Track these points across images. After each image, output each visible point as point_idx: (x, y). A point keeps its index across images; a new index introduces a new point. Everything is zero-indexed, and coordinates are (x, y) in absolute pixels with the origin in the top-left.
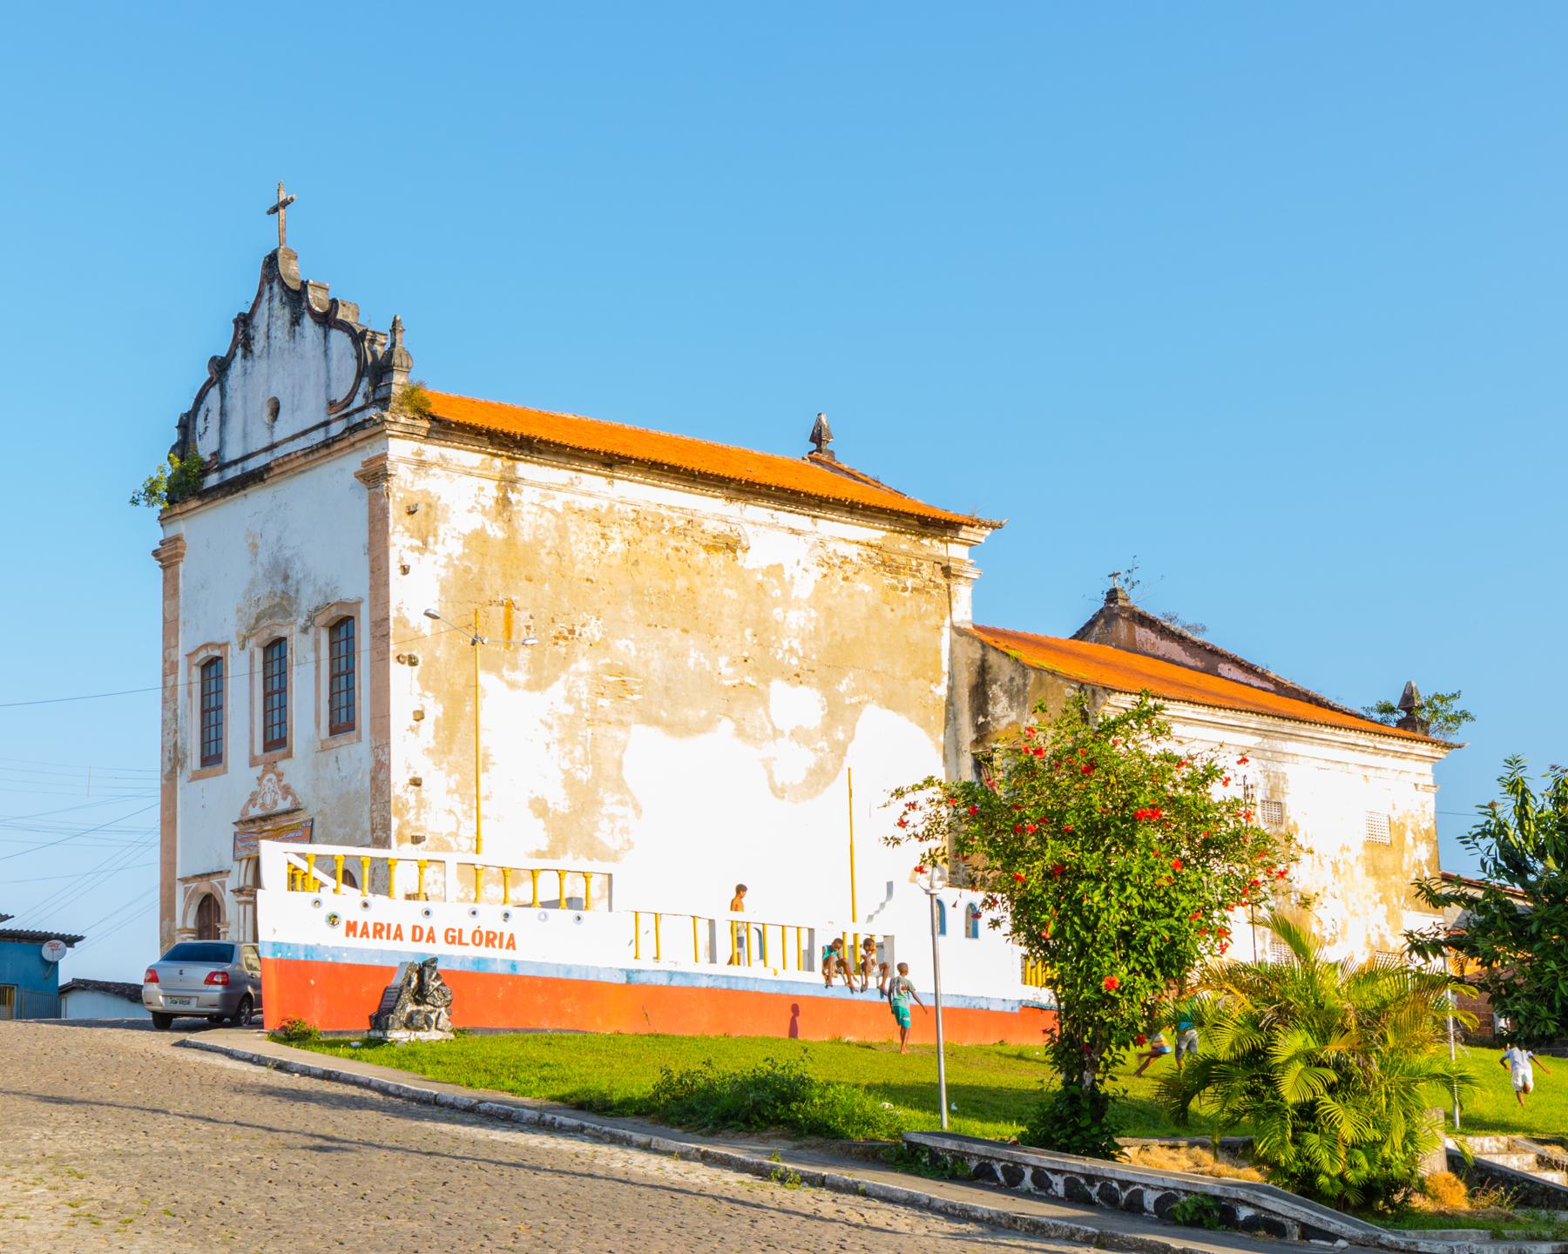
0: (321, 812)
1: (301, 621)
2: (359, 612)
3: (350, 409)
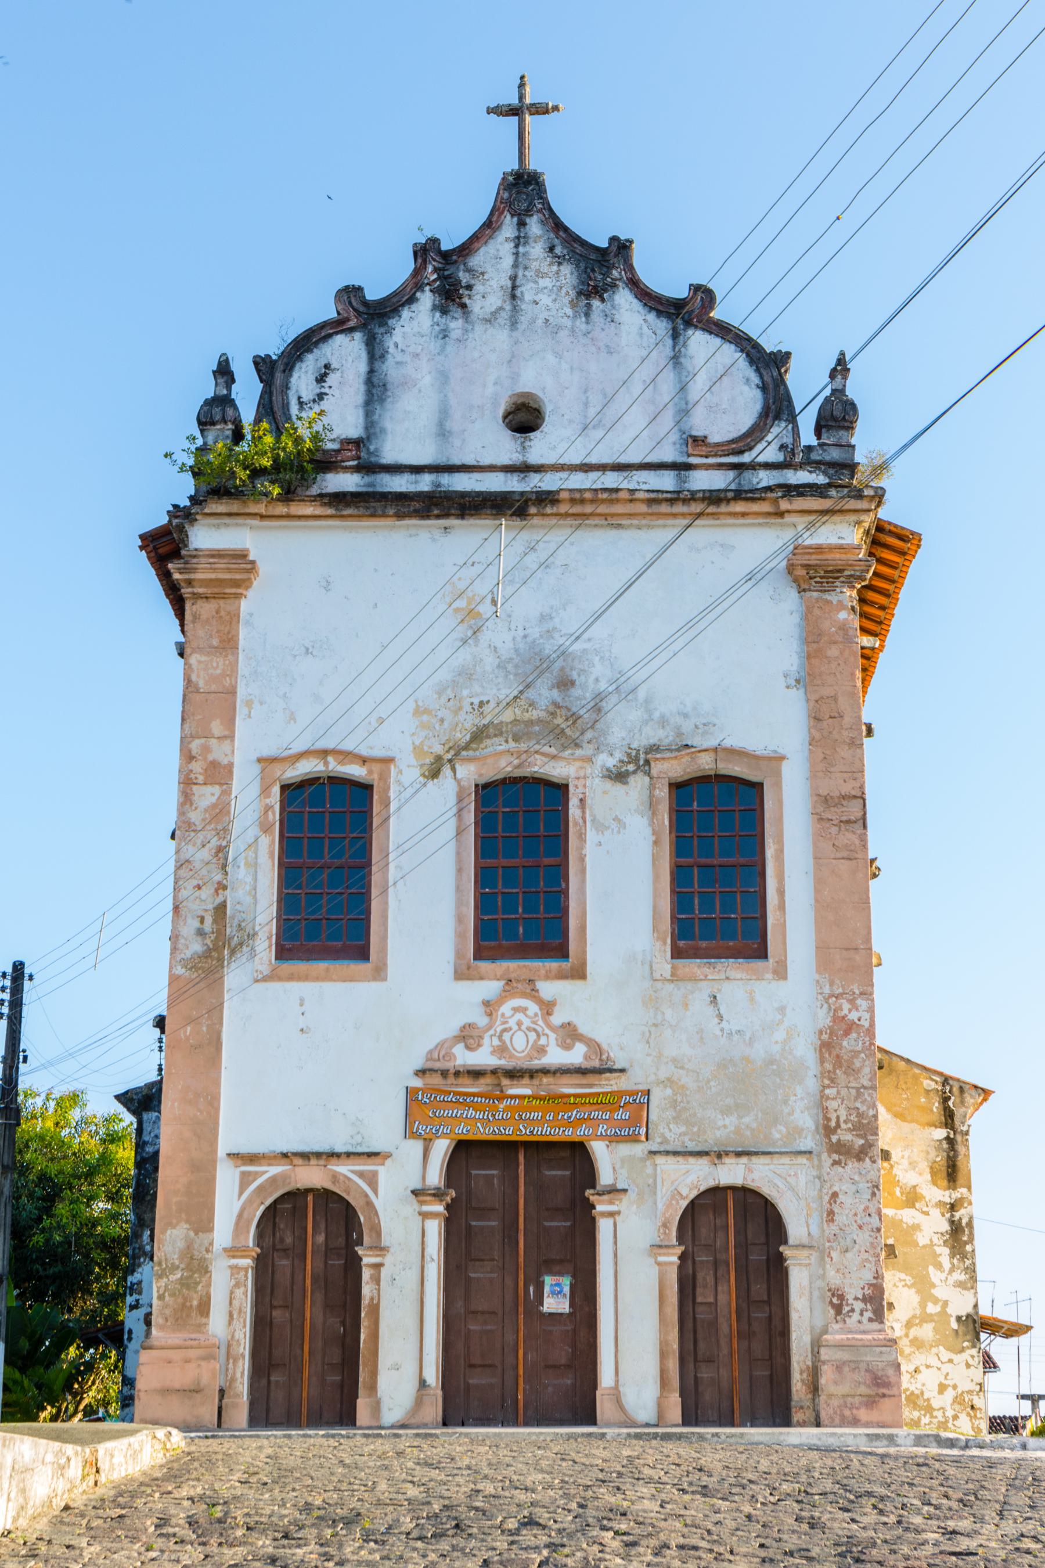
0: (669, 1082)
2: (778, 774)
3: (746, 458)
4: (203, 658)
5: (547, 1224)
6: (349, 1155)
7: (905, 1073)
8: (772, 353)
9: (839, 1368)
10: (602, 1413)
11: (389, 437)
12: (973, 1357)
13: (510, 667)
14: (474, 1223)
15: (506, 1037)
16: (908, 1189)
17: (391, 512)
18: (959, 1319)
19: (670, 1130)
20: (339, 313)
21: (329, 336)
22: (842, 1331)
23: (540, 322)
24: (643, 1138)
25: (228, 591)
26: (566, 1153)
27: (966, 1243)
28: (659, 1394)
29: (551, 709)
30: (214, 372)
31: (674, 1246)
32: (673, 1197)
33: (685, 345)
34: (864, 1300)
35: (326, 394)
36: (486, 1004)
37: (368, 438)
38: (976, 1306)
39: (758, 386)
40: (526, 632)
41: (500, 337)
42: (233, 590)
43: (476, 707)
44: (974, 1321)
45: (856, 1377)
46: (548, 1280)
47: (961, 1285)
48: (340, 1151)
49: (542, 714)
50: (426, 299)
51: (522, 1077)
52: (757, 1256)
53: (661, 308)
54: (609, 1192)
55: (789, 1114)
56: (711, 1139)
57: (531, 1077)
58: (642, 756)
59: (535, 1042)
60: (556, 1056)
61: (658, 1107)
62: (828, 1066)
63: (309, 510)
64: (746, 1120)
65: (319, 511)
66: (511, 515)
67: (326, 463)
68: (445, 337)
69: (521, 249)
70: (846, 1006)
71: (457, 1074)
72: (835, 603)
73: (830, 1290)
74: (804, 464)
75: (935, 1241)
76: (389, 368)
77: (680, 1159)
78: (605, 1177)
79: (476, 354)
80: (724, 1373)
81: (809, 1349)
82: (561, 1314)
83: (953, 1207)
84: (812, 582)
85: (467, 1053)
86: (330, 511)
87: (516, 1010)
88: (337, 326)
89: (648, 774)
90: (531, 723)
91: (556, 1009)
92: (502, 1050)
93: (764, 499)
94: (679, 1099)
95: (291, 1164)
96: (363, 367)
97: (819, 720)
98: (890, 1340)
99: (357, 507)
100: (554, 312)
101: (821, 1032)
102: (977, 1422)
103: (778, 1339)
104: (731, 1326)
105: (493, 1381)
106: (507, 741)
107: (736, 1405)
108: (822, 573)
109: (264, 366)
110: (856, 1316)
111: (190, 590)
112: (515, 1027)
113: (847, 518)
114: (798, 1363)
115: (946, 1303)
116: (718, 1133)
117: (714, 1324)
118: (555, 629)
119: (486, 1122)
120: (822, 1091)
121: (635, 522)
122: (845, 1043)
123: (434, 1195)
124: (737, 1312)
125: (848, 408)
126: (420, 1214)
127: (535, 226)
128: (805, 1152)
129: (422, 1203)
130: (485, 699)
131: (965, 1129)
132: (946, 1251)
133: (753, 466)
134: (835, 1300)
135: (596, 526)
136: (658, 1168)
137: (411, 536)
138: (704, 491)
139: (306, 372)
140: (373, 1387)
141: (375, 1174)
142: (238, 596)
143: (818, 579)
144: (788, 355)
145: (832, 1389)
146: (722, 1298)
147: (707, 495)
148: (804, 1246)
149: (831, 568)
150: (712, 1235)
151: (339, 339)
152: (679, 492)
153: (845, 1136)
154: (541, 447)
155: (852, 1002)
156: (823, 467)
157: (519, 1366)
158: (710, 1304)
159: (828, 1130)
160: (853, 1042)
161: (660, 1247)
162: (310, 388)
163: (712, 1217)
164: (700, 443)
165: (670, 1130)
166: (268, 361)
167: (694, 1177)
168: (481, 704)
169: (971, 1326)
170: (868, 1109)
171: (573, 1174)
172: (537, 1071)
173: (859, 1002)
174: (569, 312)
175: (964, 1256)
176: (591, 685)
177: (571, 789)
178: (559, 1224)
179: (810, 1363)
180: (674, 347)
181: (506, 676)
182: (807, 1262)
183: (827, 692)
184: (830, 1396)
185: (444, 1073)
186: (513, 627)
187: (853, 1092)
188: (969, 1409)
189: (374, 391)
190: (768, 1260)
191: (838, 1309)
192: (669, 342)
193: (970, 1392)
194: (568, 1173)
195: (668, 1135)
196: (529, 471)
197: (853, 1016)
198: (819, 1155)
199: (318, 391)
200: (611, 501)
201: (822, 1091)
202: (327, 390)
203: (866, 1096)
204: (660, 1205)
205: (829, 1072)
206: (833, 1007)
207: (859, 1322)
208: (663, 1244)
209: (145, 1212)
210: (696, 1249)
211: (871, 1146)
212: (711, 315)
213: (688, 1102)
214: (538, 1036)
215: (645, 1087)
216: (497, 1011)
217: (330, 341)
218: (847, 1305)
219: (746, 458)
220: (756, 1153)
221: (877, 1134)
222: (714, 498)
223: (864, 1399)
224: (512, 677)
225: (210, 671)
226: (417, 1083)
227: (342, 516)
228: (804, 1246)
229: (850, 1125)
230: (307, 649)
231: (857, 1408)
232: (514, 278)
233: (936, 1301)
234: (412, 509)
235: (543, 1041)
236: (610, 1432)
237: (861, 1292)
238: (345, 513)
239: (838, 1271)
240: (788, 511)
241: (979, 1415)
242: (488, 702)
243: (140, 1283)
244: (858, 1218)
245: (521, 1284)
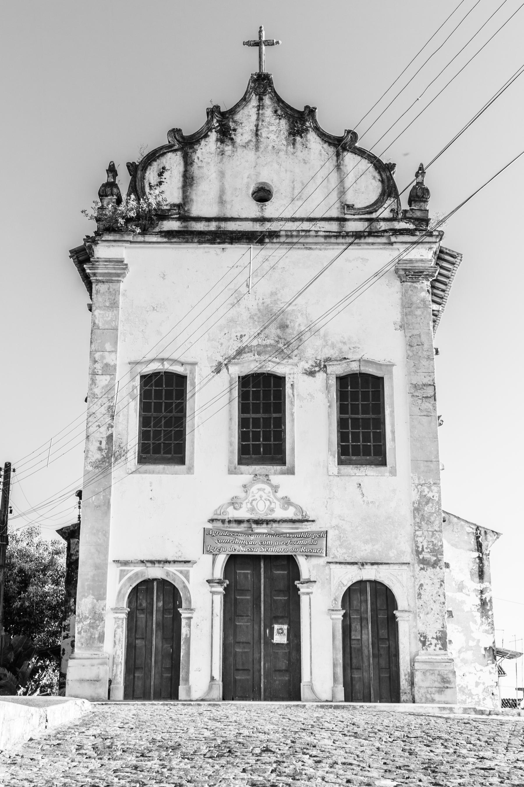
1: (307, 366)
2: (391, 373)
3: (374, 216)
4: (102, 312)
5: (275, 598)
6: (175, 562)
7: (457, 524)
8: (386, 164)
9: (424, 673)
10: (304, 695)
11: (195, 203)
12: (493, 668)
13: (256, 318)
14: (238, 597)
15: (254, 503)
16: (459, 583)
17: (196, 241)
18: (485, 649)
19: (338, 551)
20: (169, 142)
21: (165, 153)
22: (426, 654)
23: (270, 148)
24: (324, 555)
25: (114, 279)
26: (285, 563)
27: (489, 610)
28: (332, 685)
29: (277, 339)
30: (107, 170)
31: (340, 610)
32: (339, 585)
33: (343, 160)
34: (437, 639)
35: (163, 182)
36: (245, 486)
37: (184, 204)
38: (494, 642)
39: (379, 180)
40: (263, 301)
41: (250, 155)
42: (116, 279)
43: (239, 338)
44: (493, 650)
45: (433, 677)
46: (276, 627)
47: (486, 631)
48: (170, 560)
49: (272, 342)
50: (213, 136)
51: (262, 523)
52: (382, 616)
53: (330, 141)
54: (307, 582)
55: (398, 544)
56: (358, 557)
57: (267, 524)
58: (323, 363)
59: (269, 506)
60: (279, 514)
61: (331, 540)
62: (418, 520)
63: (154, 239)
64: (376, 547)
65: (160, 240)
66: (256, 243)
67: (163, 216)
68: (222, 154)
69: (261, 112)
70: (426, 490)
71: (230, 522)
72: (419, 288)
73: (419, 633)
74: (403, 219)
75: (473, 609)
76: (195, 170)
77: (343, 566)
78: (304, 575)
79: (238, 163)
80: (366, 675)
81: (409, 664)
82: (283, 644)
83: (482, 592)
84: (408, 277)
85: (235, 511)
86: (165, 240)
87: (259, 490)
88: (169, 148)
89: (326, 372)
90: (266, 346)
91: (280, 490)
92: (253, 510)
93: (383, 236)
94: (342, 536)
95: (146, 566)
96: (181, 168)
97: (411, 346)
98: (450, 659)
99: (179, 238)
100: (277, 143)
101: (414, 503)
102: (495, 702)
103: (393, 658)
104: (369, 651)
105: (248, 677)
106: (254, 355)
107: (372, 692)
108: (413, 273)
109: (132, 168)
110: (433, 647)
111: (95, 278)
112: (259, 499)
113: (425, 246)
114: (404, 670)
115: (479, 641)
116: (362, 553)
117: (360, 650)
118: (278, 299)
119: (244, 545)
120: (415, 533)
121: (318, 247)
122: (426, 509)
123: (218, 583)
124: (372, 644)
125: (425, 191)
126: (211, 592)
127: (267, 101)
128: (406, 563)
129: (212, 587)
130: (243, 334)
131: (487, 552)
132: (479, 614)
133: (378, 220)
134: (422, 639)
135: (299, 248)
136: (332, 570)
137: (206, 252)
138: (353, 232)
139: (153, 171)
140: (187, 680)
141: (188, 572)
142: (119, 281)
143: (410, 276)
144: (394, 165)
145: (421, 684)
146: (364, 637)
147: (354, 234)
148: (406, 611)
149: (417, 271)
150: (359, 605)
151: (170, 155)
152: (340, 232)
153: (426, 555)
154: (271, 209)
155: (429, 487)
156: (412, 221)
157: (261, 671)
158: (358, 640)
159: (418, 553)
160: (430, 508)
161: (333, 610)
162: (155, 179)
163: (359, 595)
164: (351, 208)
165: (338, 551)
166: (134, 165)
167: (351, 576)
168: (241, 336)
169: (492, 653)
170: (438, 542)
171: (289, 573)
172: (270, 521)
173: (433, 488)
174: (285, 143)
175: (488, 617)
176: (297, 328)
177: (287, 379)
178: (282, 598)
179: (409, 671)
180: (337, 161)
181: (254, 323)
182: (408, 619)
183: (416, 332)
184: (420, 687)
185: (223, 521)
186: (257, 298)
187: (430, 533)
188: (491, 695)
189: (187, 181)
190: (388, 618)
191: (424, 643)
192: (335, 158)
193: (491, 686)
194: (286, 572)
195: (336, 553)
196: (265, 221)
197: (430, 495)
198: (413, 565)
199: (159, 180)
200: (306, 236)
201: (415, 533)
202: (163, 180)
203: (437, 535)
204: (332, 589)
205: (418, 523)
206: (420, 490)
207: (435, 650)
208: (335, 609)
209: (71, 589)
210: (351, 611)
211: (440, 561)
212: (356, 145)
213: (347, 537)
214: (271, 503)
215: (324, 529)
216: (250, 490)
217: (165, 156)
218: (428, 641)
219: (374, 216)
220: (381, 564)
221: (442, 555)
222: (358, 235)
223: (438, 689)
224: (256, 323)
225: (105, 319)
226: (210, 526)
227: (171, 242)
228: (406, 611)
229: (429, 550)
230: (154, 308)
231: (434, 694)
232: (257, 126)
233: (474, 639)
234: (206, 239)
235: (273, 506)
236: (308, 704)
237: (436, 635)
238: (173, 241)
239: (423, 624)
240: (395, 242)
241: (496, 698)
242: (245, 335)
243: (69, 625)
244: (433, 597)
245: (262, 628)
